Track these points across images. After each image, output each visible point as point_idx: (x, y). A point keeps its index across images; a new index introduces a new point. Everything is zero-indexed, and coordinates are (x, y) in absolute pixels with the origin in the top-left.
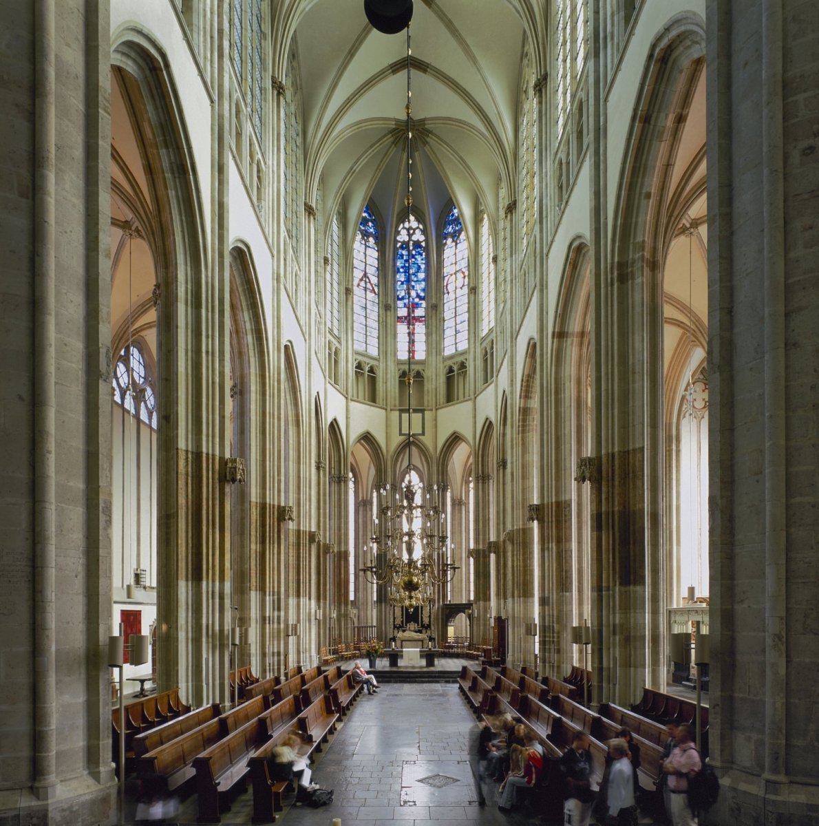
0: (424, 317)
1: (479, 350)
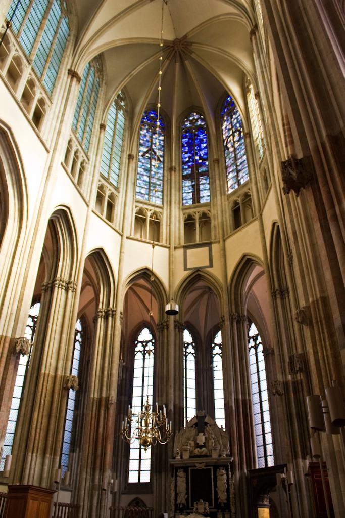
0: (208, 171)
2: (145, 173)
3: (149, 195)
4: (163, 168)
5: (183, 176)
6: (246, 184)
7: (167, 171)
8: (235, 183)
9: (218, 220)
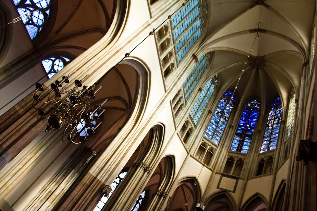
1: (282, 148)
2: (215, 124)
3: (212, 136)
4: (226, 125)
5: (236, 133)
6: (273, 151)
7: (228, 127)
8: (266, 148)
9: (248, 166)
